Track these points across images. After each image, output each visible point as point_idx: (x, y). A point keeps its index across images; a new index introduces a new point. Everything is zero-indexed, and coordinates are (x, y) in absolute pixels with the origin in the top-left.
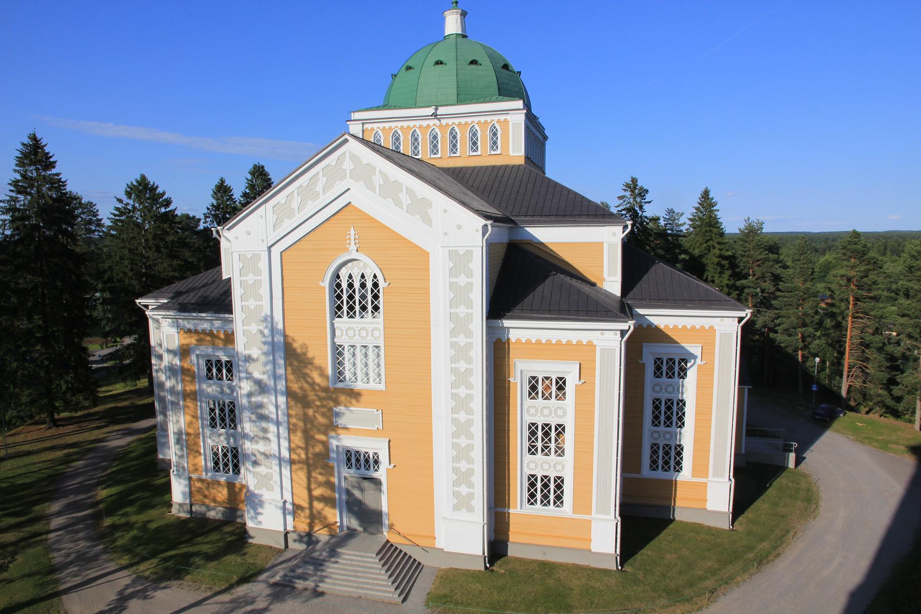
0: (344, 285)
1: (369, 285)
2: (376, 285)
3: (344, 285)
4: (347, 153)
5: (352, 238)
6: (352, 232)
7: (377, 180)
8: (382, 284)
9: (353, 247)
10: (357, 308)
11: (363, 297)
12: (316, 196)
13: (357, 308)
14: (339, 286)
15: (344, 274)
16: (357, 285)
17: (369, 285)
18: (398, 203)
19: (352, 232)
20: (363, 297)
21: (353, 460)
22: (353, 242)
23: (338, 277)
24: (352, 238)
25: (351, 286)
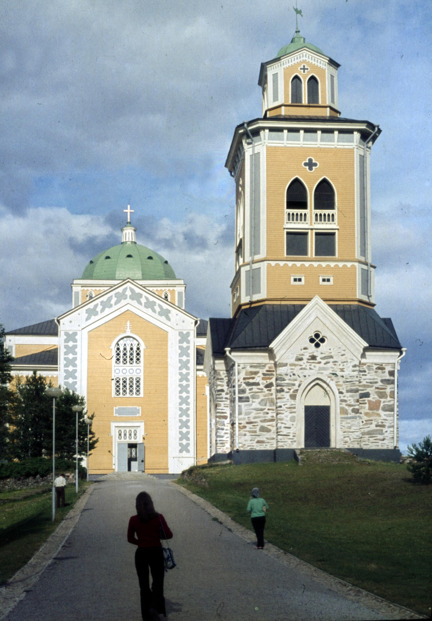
0: (122, 349)
1: (135, 349)
2: (138, 349)
3: (122, 349)
4: (128, 288)
5: (128, 326)
6: (128, 323)
7: (143, 300)
8: (142, 348)
9: (128, 330)
10: (128, 359)
11: (131, 354)
12: (111, 306)
13: (128, 359)
14: (118, 349)
15: (121, 342)
16: (128, 349)
17: (135, 349)
18: (154, 311)
19: (128, 323)
20: (131, 354)
21: (123, 435)
22: (128, 328)
23: (118, 345)
24: (128, 326)
25: (125, 349)
